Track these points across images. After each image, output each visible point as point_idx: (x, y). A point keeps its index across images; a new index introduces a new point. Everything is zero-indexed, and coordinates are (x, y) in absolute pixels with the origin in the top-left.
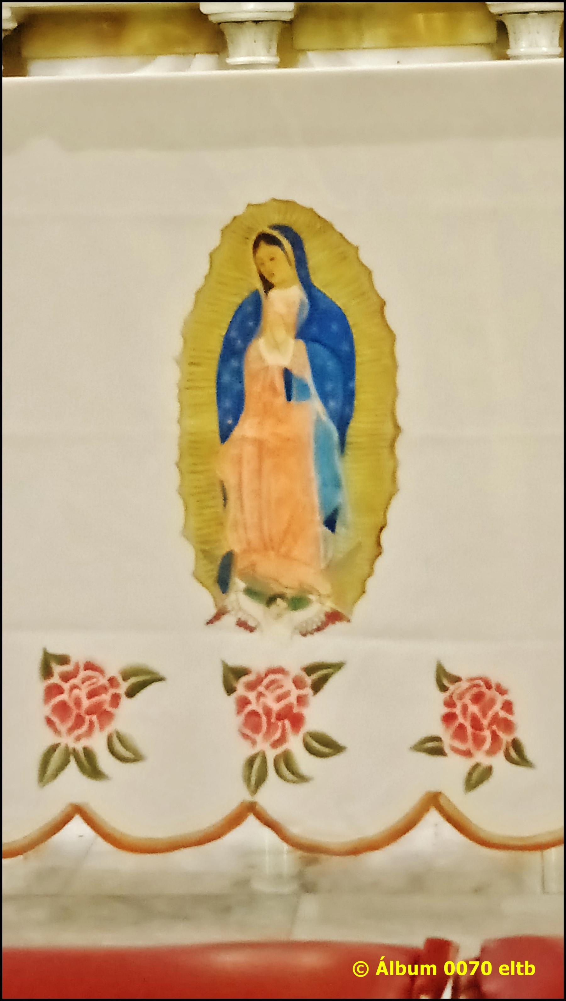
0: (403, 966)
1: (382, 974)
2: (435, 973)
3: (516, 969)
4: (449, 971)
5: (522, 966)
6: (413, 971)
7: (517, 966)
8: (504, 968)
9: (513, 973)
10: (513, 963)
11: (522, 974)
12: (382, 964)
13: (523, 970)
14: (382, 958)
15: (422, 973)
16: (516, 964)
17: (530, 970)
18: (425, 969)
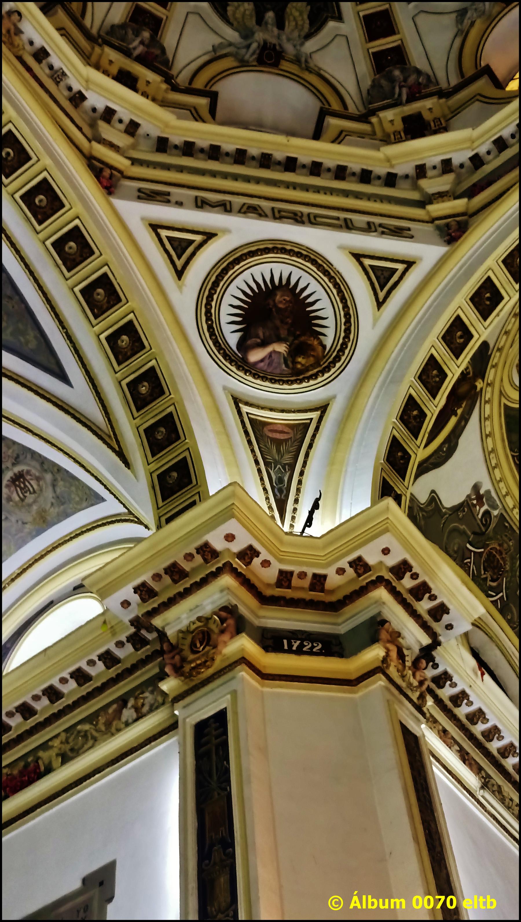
0: (375, 900)
1: (356, 907)
2: (404, 907)
3: (478, 903)
4: (417, 904)
5: (485, 900)
6: (384, 905)
7: (479, 900)
8: (468, 902)
9: (476, 907)
10: (476, 897)
11: (484, 908)
12: (355, 898)
13: (485, 904)
14: (356, 892)
16: (478, 898)
17: (492, 904)
18: (395, 903)
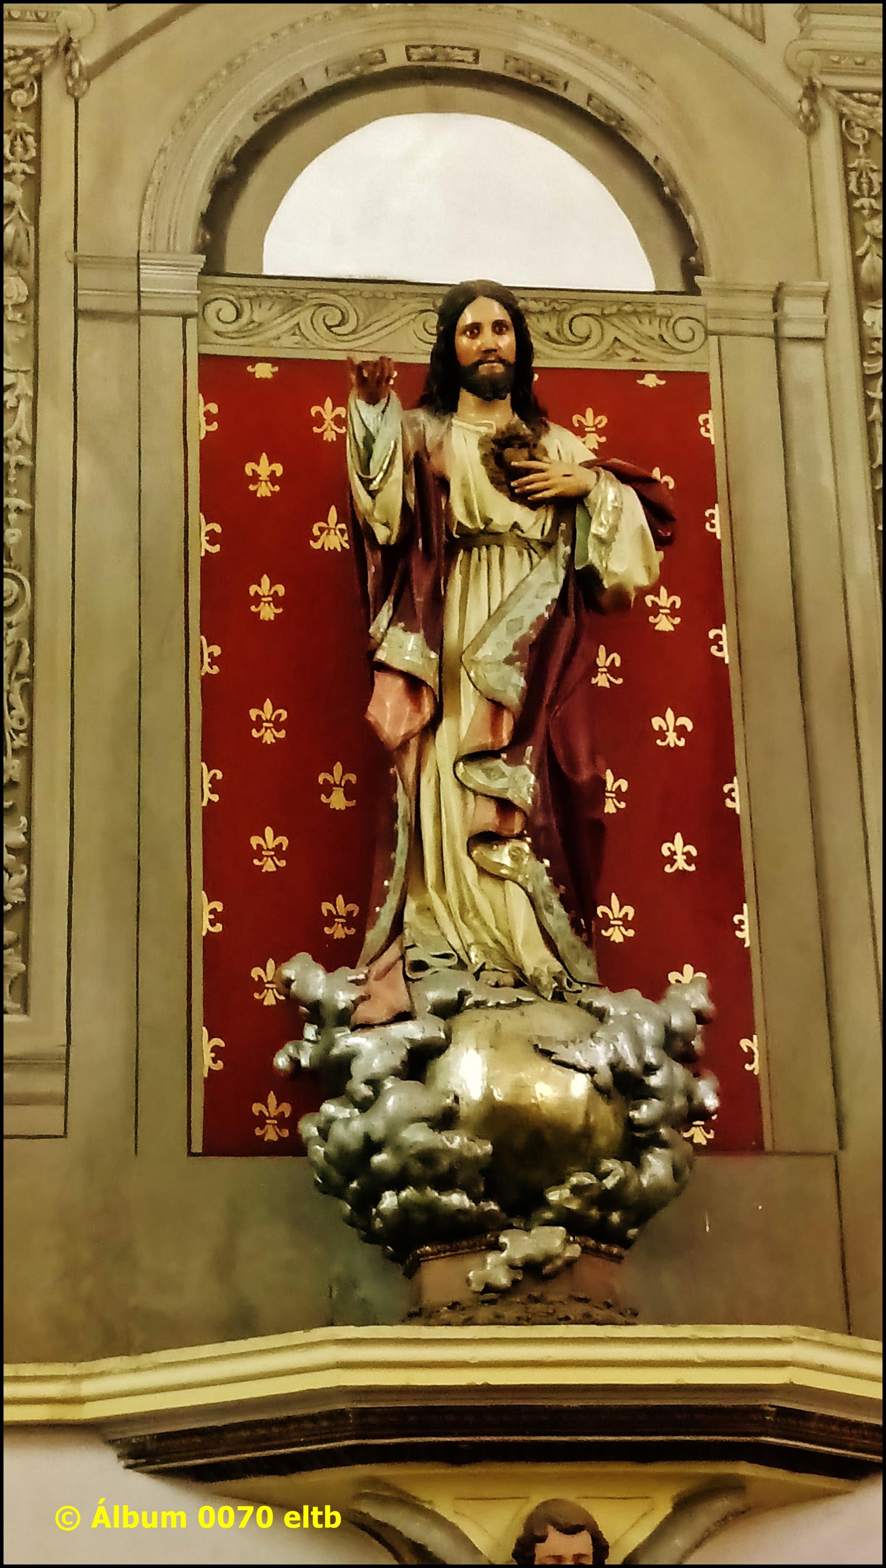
0: (134, 1514)
1: (101, 1526)
2: (183, 1525)
3: (311, 1517)
4: (207, 1520)
5: (321, 1513)
6: (150, 1520)
7: (312, 1513)
8: (292, 1516)
9: (306, 1525)
11: (321, 1526)
12: (101, 1510)
13: (321, 1519)
14: (102, 1500)
15: (164, 1525)
16: (310, 1510)
18: (169, 1518)
